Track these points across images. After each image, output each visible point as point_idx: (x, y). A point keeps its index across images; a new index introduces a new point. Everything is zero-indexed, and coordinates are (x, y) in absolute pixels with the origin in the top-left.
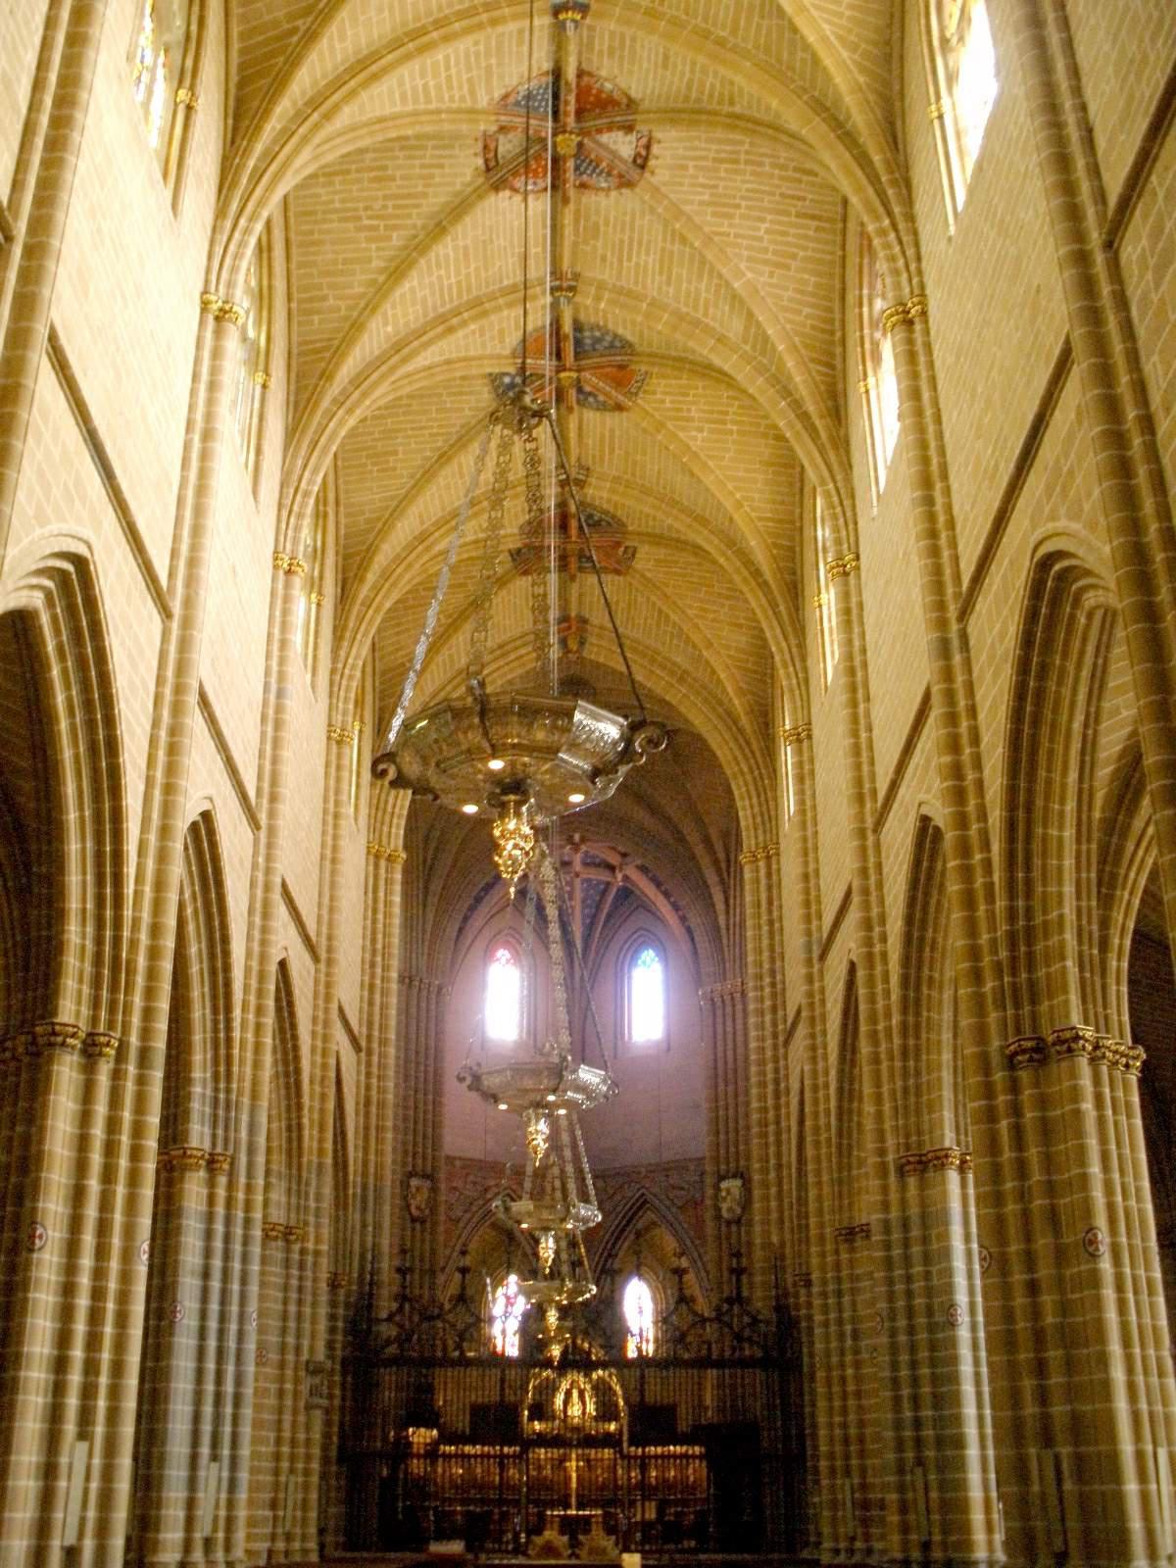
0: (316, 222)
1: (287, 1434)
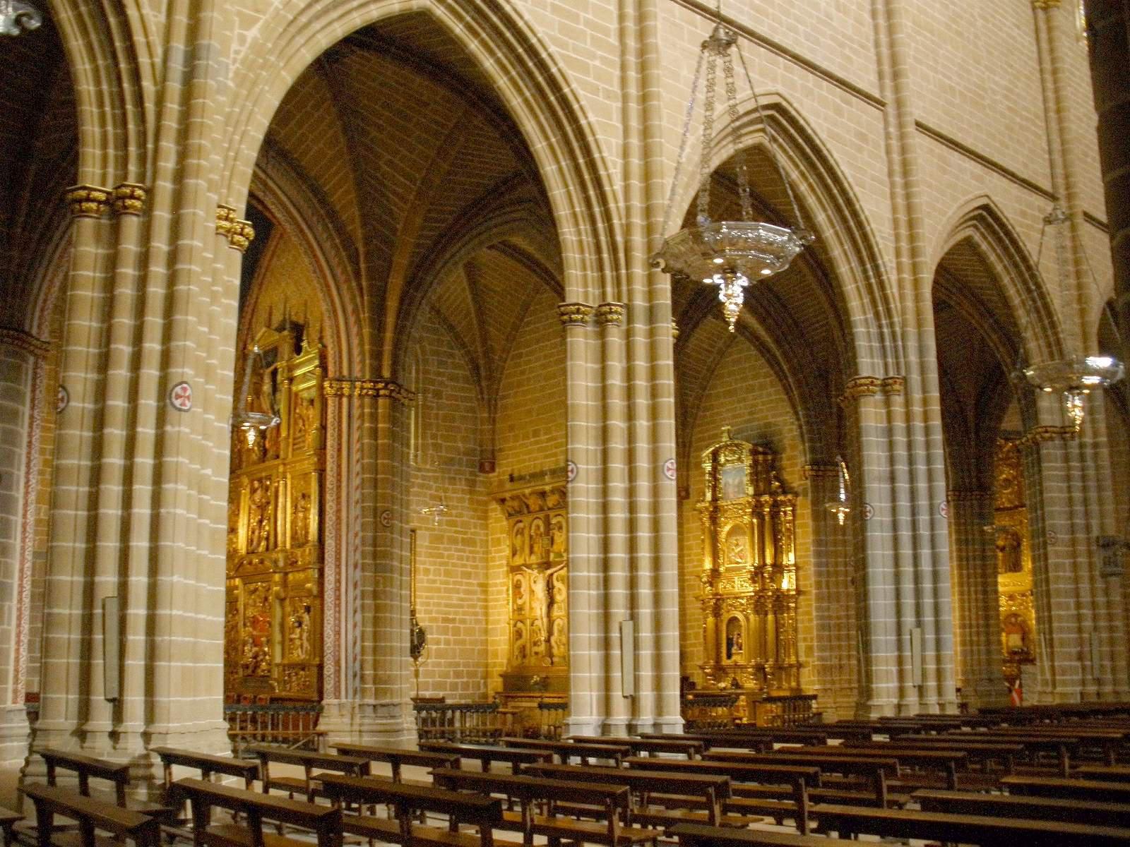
1: (1086, 598)
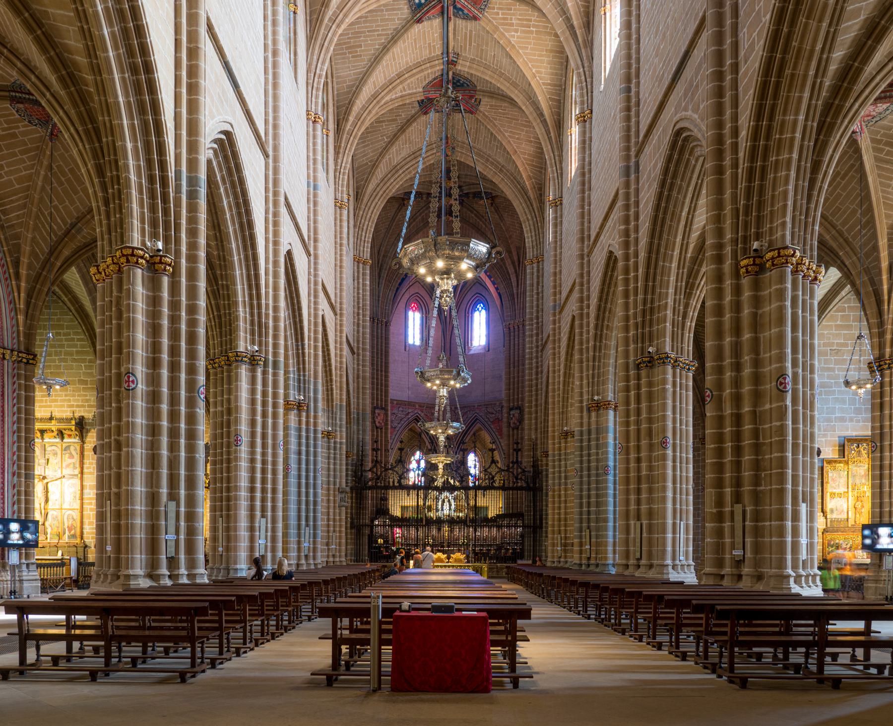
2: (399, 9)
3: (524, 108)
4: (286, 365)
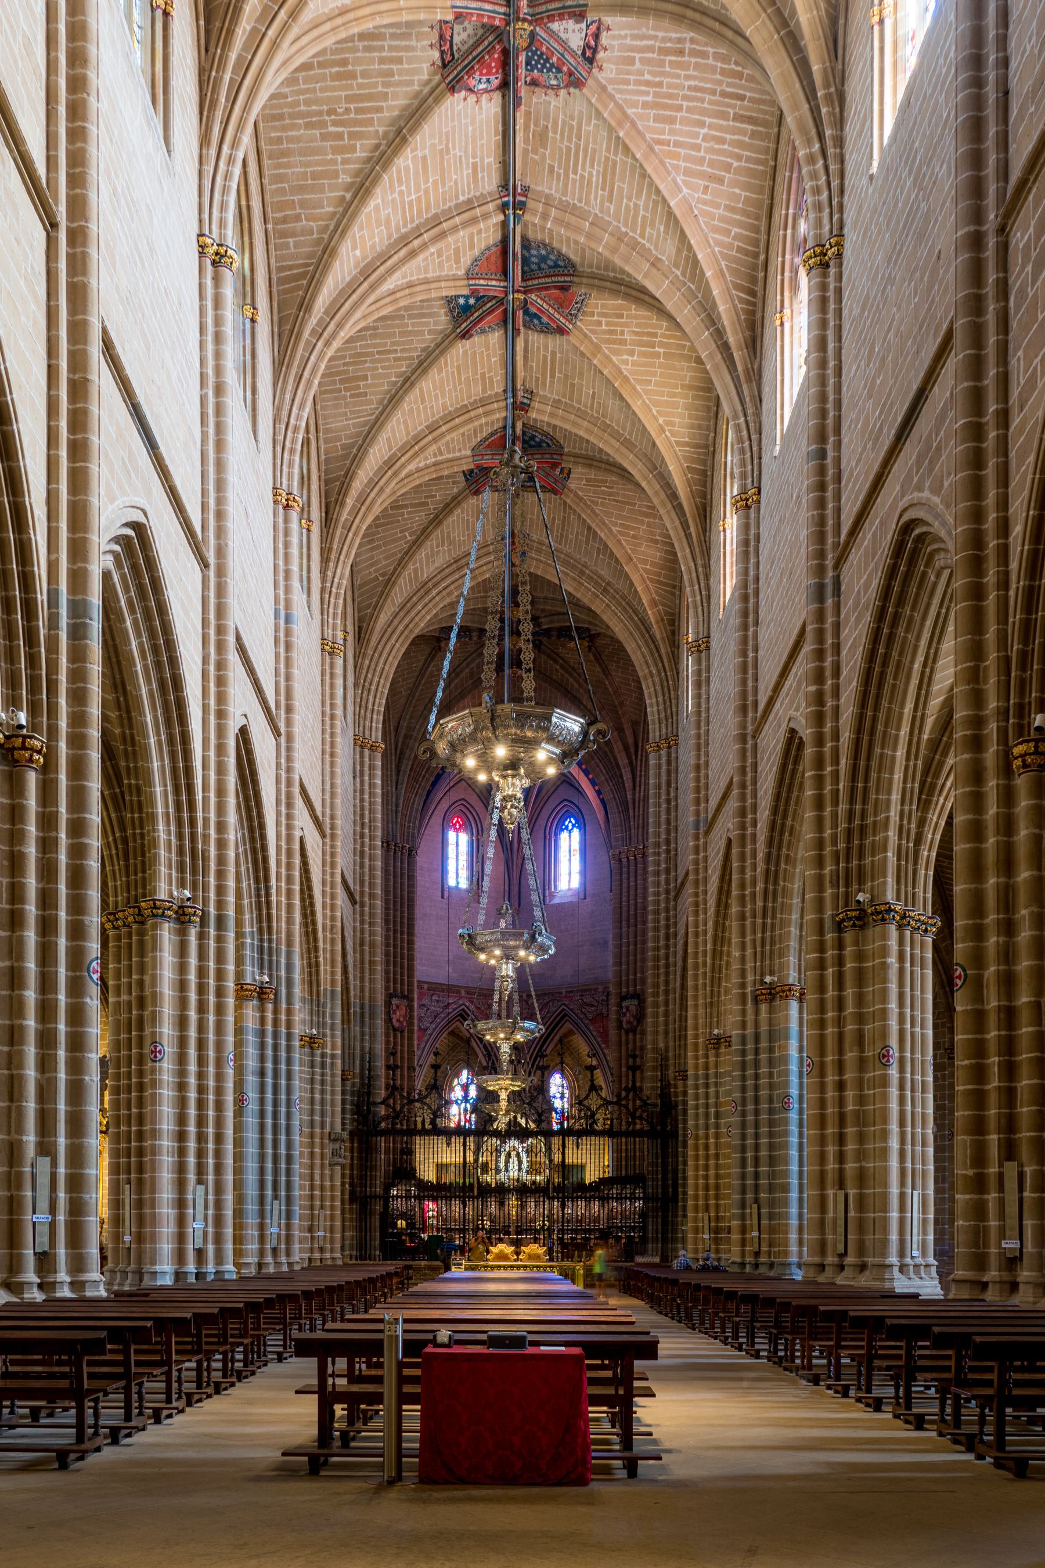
0: (284, 129)
2: (430, 315)
3: (644, 484)
4: (239, 923)
